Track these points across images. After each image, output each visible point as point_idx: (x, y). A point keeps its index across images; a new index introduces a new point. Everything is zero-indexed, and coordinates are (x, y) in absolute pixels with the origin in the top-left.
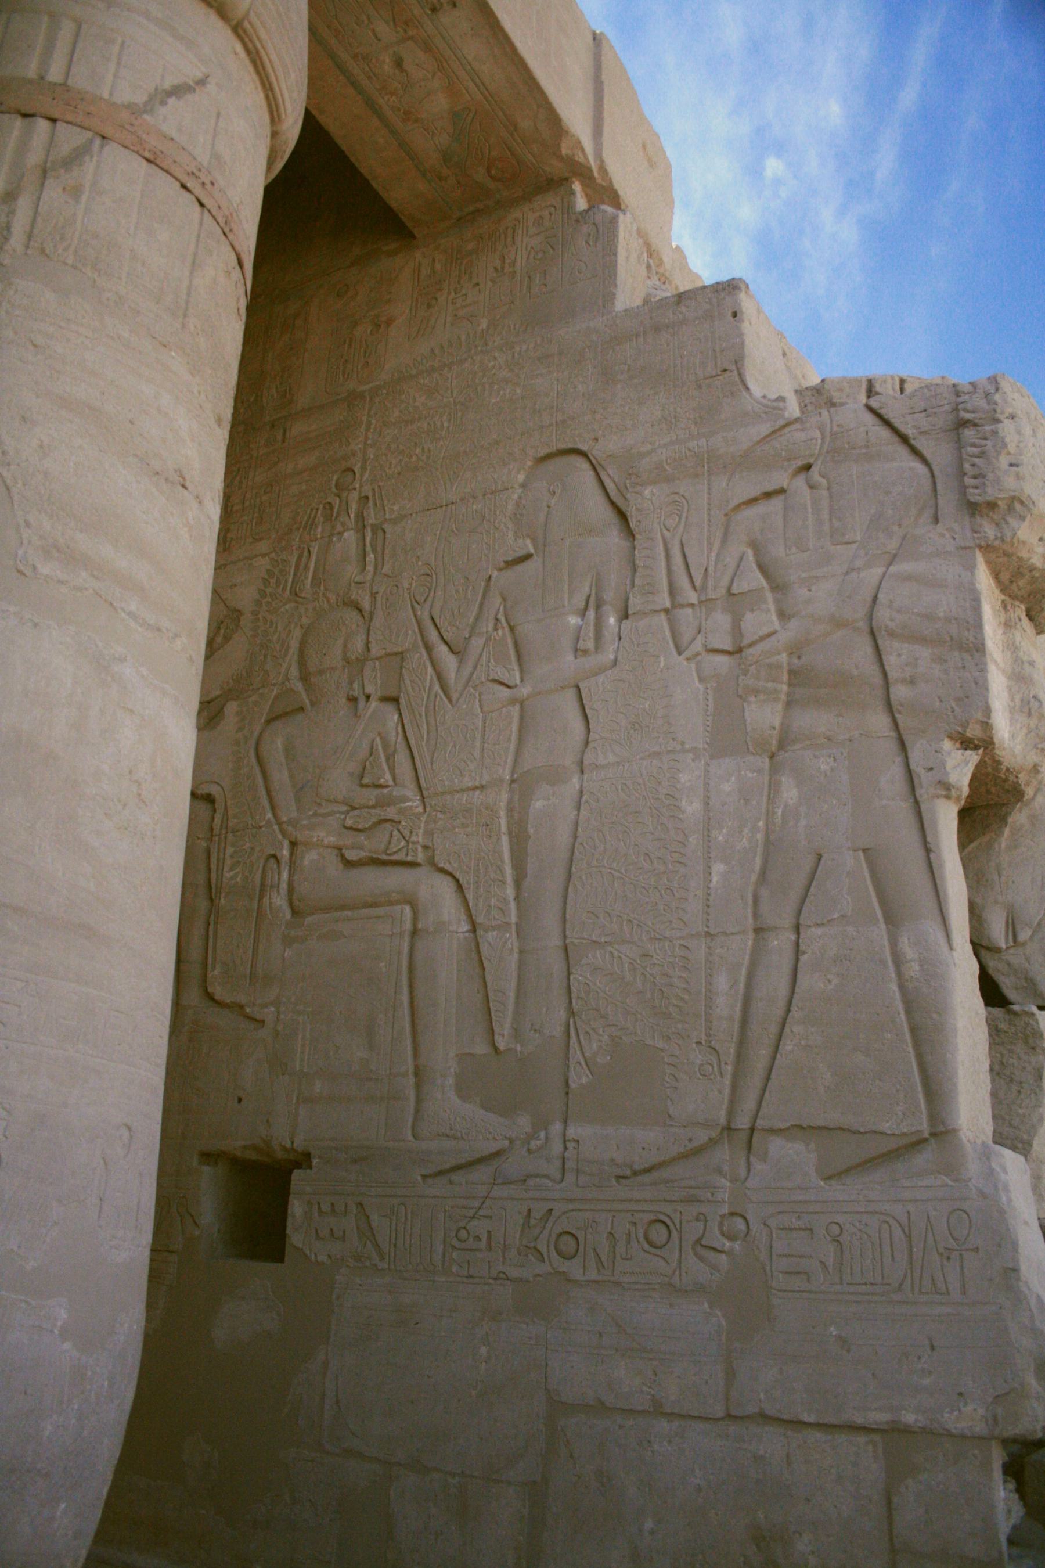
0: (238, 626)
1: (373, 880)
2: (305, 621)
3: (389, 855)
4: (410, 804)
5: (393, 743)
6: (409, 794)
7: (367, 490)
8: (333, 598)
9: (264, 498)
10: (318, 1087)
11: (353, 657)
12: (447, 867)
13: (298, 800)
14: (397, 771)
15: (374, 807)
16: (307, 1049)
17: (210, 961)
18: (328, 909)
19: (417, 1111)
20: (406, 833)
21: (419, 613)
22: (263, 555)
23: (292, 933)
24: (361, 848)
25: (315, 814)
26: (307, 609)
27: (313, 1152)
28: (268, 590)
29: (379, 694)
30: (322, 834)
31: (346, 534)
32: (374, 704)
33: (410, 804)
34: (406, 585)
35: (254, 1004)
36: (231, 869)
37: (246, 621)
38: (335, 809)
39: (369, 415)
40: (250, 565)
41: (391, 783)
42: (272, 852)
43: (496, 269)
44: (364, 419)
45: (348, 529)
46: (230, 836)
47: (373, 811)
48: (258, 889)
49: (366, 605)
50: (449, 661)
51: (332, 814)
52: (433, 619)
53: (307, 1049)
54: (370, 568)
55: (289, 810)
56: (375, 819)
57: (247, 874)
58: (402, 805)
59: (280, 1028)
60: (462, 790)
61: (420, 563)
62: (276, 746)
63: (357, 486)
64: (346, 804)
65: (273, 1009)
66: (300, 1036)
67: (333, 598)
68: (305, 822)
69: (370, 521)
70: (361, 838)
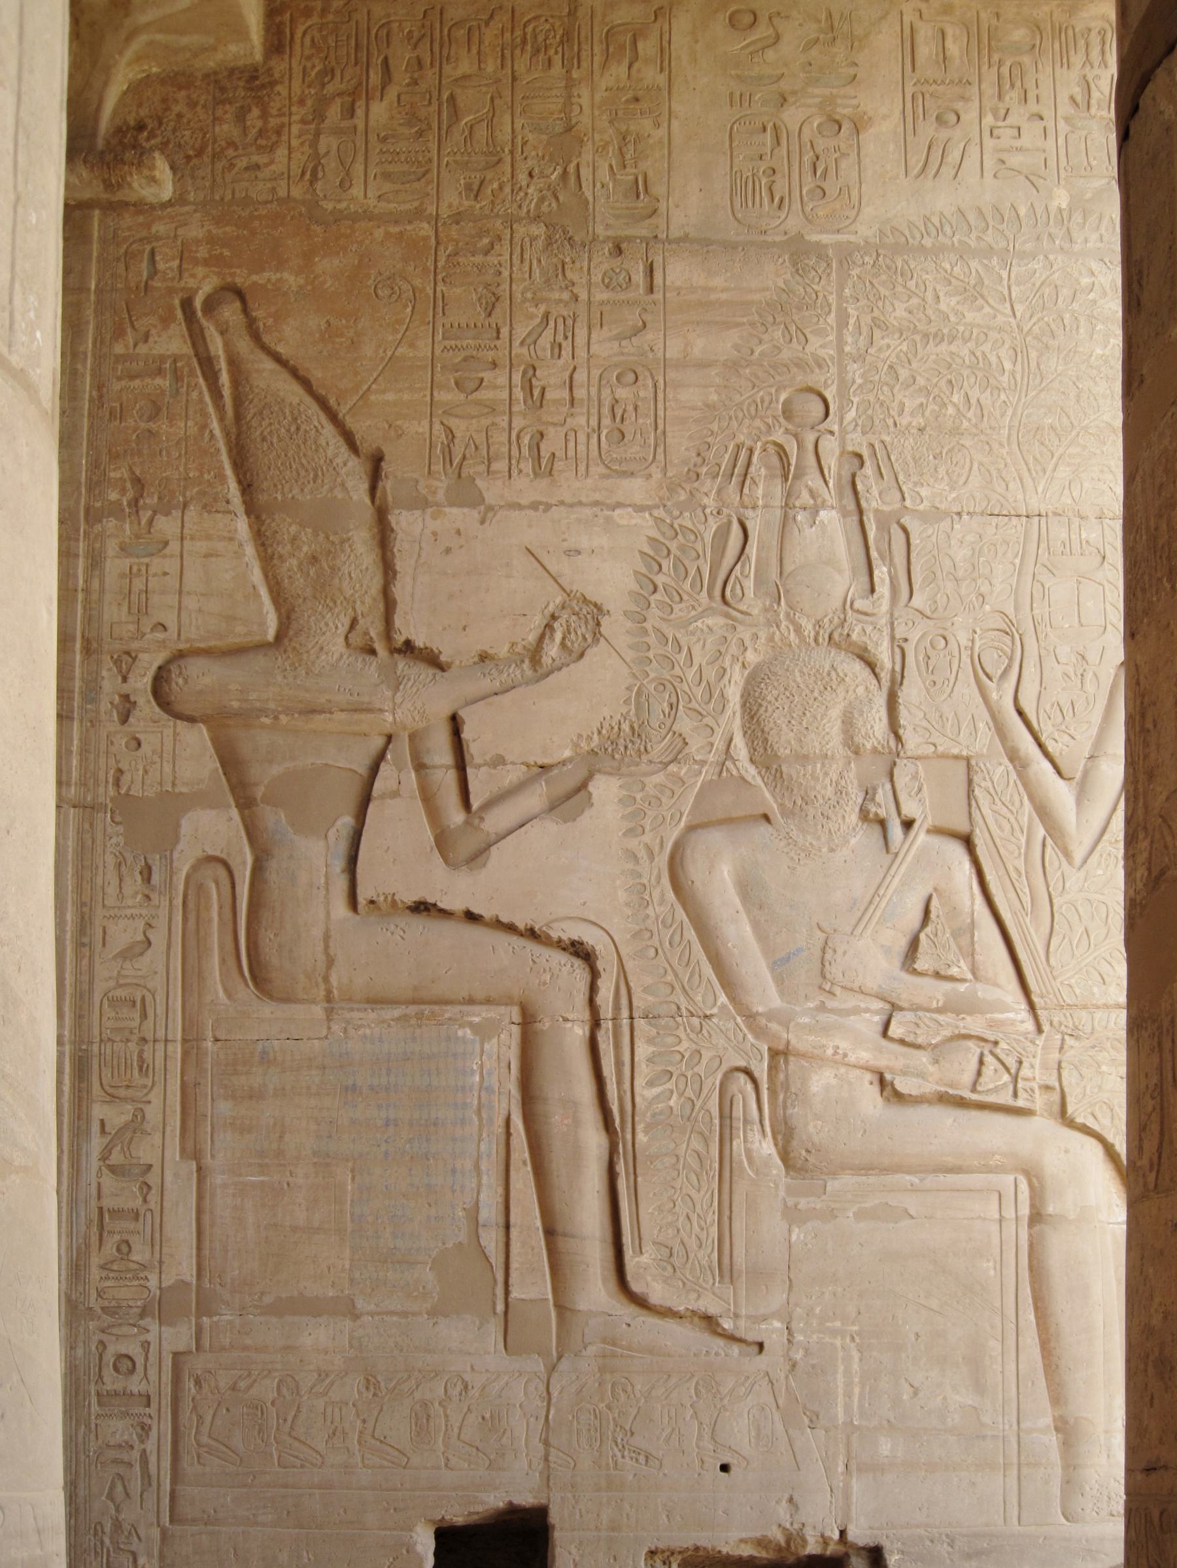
0: (597, 635)
1: (949, 1131)
2: (751, 657)
3: (979, 1092)
4: (1011, 1015)
5: (967, 910)
6: (1009, 999)
7: (857, 441)
8: (808, 628)
9: (622, 393)
10: (885, 1447)
11: (869, 746)
12: (1091, 1123)
13: (779, 981)
14: (977, 957)
15: (938, 1010)
16: (857, 1390)
17: (627, 1239)
18: (866, 1169)
19: (1067, 1482)
20: (1011, 1062)
21: (994, 696)
22: (640, 509)
23: (803, 1203)
24: (922, 1075)
25: (822, 1008)
26: (755, 637)
27: (886, 1545)
28: (660, 580)
29: (929, 822)
30: (844, 1045)
31: (823, 514)
32: (920, 837)
33: (1011, 1015)
34: (964, 642)
35: (736, 1316)
36: (651, 1084)
37: (615, 627)
38: (863, 1005)
39: (840, 296)
40: (608, 520)
41: (969, 976)
42: (742, 1063)
43: (1072, 99)
44: (832, 299)
45: (823, 506)
46: (640, 1023)
47: (941, 1018)
48: (717, 1121)
49: (884, 655)
50: (1061, 794)
51: (856, 1011)
52: (1020, 713)
53: (857, 1390)
54: (883, 589)
55: (765, 995)
56: (947, 1033)
57: (689, 1093)
58: (997, 1016)
59: (798, 1355)
60: (1106, 1006)
61: (987, 607)
62: (719, 874)
63: (836, 428)
64: (884, 999)
65: (777, 1324)
66: (841, 1369)
67: (808, 628)
68: (805, 1020)
69: (874, 504)
70: (923, 1058)
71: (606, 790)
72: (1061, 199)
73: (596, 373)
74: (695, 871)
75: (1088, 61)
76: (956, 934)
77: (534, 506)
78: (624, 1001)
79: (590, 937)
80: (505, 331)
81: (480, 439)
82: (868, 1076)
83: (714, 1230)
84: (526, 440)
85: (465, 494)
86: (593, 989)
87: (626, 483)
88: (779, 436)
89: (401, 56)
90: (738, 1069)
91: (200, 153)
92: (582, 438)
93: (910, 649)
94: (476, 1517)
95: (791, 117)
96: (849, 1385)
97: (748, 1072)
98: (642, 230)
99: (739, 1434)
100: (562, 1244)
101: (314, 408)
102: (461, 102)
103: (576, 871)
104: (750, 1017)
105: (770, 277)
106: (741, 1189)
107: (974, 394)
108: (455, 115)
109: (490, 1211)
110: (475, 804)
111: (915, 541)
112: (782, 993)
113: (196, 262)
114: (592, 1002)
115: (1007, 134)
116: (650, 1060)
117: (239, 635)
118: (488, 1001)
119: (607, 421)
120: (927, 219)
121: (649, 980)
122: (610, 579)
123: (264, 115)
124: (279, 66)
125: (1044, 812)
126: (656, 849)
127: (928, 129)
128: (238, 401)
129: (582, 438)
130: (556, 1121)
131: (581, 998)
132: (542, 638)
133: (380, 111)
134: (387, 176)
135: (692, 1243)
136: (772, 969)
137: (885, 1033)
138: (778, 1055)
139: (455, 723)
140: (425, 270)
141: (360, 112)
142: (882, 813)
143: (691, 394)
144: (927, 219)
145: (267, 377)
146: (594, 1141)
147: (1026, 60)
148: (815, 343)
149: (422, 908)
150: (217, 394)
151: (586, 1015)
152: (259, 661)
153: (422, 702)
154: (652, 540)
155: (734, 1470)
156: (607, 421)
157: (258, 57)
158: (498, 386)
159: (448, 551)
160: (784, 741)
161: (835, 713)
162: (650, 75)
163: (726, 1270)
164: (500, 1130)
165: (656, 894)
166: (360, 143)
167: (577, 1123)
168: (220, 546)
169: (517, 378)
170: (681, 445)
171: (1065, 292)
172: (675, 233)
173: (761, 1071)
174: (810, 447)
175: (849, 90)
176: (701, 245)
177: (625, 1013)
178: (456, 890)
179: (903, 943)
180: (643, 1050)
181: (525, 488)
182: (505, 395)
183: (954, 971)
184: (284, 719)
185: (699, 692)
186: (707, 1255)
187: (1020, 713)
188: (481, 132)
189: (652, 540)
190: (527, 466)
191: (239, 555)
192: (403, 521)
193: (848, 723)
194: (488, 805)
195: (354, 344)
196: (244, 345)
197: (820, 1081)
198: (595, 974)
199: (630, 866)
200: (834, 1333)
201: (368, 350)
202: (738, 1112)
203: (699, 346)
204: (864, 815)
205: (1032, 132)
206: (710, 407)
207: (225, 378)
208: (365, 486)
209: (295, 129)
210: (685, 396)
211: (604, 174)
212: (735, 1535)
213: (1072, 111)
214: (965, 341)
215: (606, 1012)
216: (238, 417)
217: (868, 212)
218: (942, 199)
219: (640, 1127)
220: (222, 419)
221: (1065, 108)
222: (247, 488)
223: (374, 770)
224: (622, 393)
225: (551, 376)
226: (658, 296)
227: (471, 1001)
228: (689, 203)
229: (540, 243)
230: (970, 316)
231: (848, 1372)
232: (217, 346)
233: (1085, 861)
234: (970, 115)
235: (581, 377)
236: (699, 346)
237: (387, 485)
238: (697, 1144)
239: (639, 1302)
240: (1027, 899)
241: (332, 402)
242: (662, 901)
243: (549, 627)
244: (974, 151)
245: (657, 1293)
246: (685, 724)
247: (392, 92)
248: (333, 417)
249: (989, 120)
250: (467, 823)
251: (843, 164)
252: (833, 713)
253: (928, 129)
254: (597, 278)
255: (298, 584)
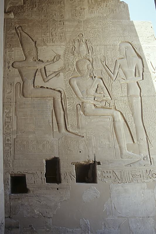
9: (61, 34)
13: (82, 94)
21: (103, 63)
22: (64, 45)
27: (100, 161)
28: (66, 52)
32: (96, 78)
34: (99, 58)
36: (68, 106)
44: (83, 25)
49: (91, 59)
51: (91, 97)
52: (106, 65)
54: (90, 53)
55: (80, 95)
62: (75, 83)
67: (82, 57)
71: (61, 74)
72: (105, 15)
73: (58, 33)
74: (72, 82)
75: (106, 2)
76: (101, 89)
77: (53, 46)
78: (65, 97)
79: (61, 90)
80: (49, 29)
81: (47, 39)
82: (93, 105)
83: (77, 123)
84: (51, 39)
85: (46, 45)
86: (61, 95)
87: (62, 43)
88: (78, 38)
89: (37, 4)
90: (78, 104)
91: (16, 14)
92: (57, 39)
93: (93, 59)
94: (50, 159)
95: (77, 8)
96: (94, 141)
97: (79, 104)
98: (63, 19)
99: (82, 148)
100: (59, 125)
101: (29, 37)
102: (43, 8)
103: (59, 83)
104: (79, 98)
105: (76, 23)
106: (79, 118)
107: (98, 34)
108: (43, 10)
109: (51, 121)
110: (47, 76)
111: (93, 48)
112: (82, 95)
113: (16, 24)
114: (61, 97)
115: (99, 9)
116: (68, 103)
117: (21, 59)
118: (49, 97)
119: (60, 37)
120: (92, 18)
121: (67, 94)
122: (61, 52)
123: (23, 10)
124: (25, 5)
125: (110, 75)
126: (67, 80)
127: (91, 9)
128: (21, 37)
129: (57, 39)
130: (58, 110)
131: (60, 96)
132: (54, 59)
133: (35, 9)
134: (36, 15)
135: (74, 124)
136: (81, 93)
137: (94, 100)
138: (83, 103)
139: (45, 68)
140: (40, 24)
141: (33, 9)
142: (92, 76)
143: (68, 35)
144: (92, 18)
145: (24, 34)
146: (62, 112)
147: (100, 2)
148: (81, 29)
149: (41, 87)
150: (19, 36)
151: (61, 98)
152: (24, 62)
153: (41, 66)
154: (65, 49)
155: (81, 152)
156: (60, 37)
157: (23, 4)
158: (48, 34)
159: (43, 50)
160: (81, 69)
161: (86, 65)
162: (63, 5)
163: (78, 127)
164: (51, 111)
165: (68, 85)
166: (33, 12)
167: (60, 110)
168: (19, 51)
169: (50, 33)
170: (68, 39)
171: (106, 24)
172: (66, 19)
173: (81, 105)
174: (81, 39)
175: (83, 6)
176: (68, 20)
177: (65, 98)
178: (46, 85)
179: (95, 90)
180: (67, 102)
181: (51, 44)
182: (49, 35)
183: (102, 93)
184: (26, 68)
185: (71, 63)
186: (76, 126)
187: (106, 65)
188: (46, 11)
189: (65, 49)
190: (52, 42)
191: (21, 51)
192: (39, 48)
193: (87, 66)
194: (49, 76)
195: (33, 31)
196: (21, 31)
197: (88, 105)
198: (61, 94)
199: (65, 82)
200: (92, 135)
201: (34, 31)
202: (79, 109)
203: (69, 30)
204: (90, 76)
205: (101, 9)
206: (70, 36)
207: (19, 35)
208: (34, 45)
209: (26, 11)
210: (68, 34)
211: (58, 14)
212: (82, 160)
213: (105, 7)
214: (97, 29)
215: (63, 98)
216: (21, 38)
217: (85, 17)
218: (93, 15)
219: (67, 111)
220: (19, 39)
221: (105, 7)
222: (22, 45)
223: (36, 73)
224: (61, 34)
225: (54, 33)
226: (65, 25)
227: (48, 97)
228: (67, 16)
229: (52, 21)
230: (97, 26)
231: (94, 140)
232: (18, 32)
233: (115, 80)
234: (95, 8)
235: (57, 33)
236: (69, 30)
237: (37, 44)
238: (74, 112)
239: (69, 132)
240: (109, 85)
241: (31, 36)
242: (69, 86)
243: (55, 57)
244: (96, 11)
245: (71, 130)
246: (70, 67)
247: (36, 7)
248: (31, 38)
249: (97, 8)
250: (46, 78)
251: (83, 13)
252: (85, 66)
253: (91, 9)
254: (58, 24)
255: (27, 54)
